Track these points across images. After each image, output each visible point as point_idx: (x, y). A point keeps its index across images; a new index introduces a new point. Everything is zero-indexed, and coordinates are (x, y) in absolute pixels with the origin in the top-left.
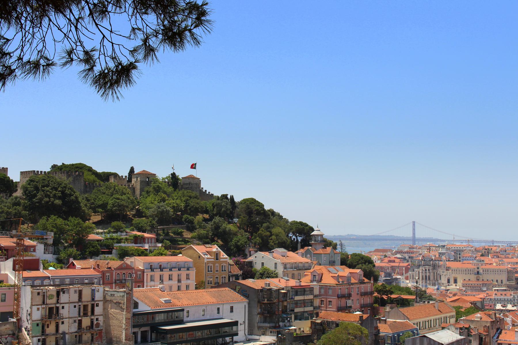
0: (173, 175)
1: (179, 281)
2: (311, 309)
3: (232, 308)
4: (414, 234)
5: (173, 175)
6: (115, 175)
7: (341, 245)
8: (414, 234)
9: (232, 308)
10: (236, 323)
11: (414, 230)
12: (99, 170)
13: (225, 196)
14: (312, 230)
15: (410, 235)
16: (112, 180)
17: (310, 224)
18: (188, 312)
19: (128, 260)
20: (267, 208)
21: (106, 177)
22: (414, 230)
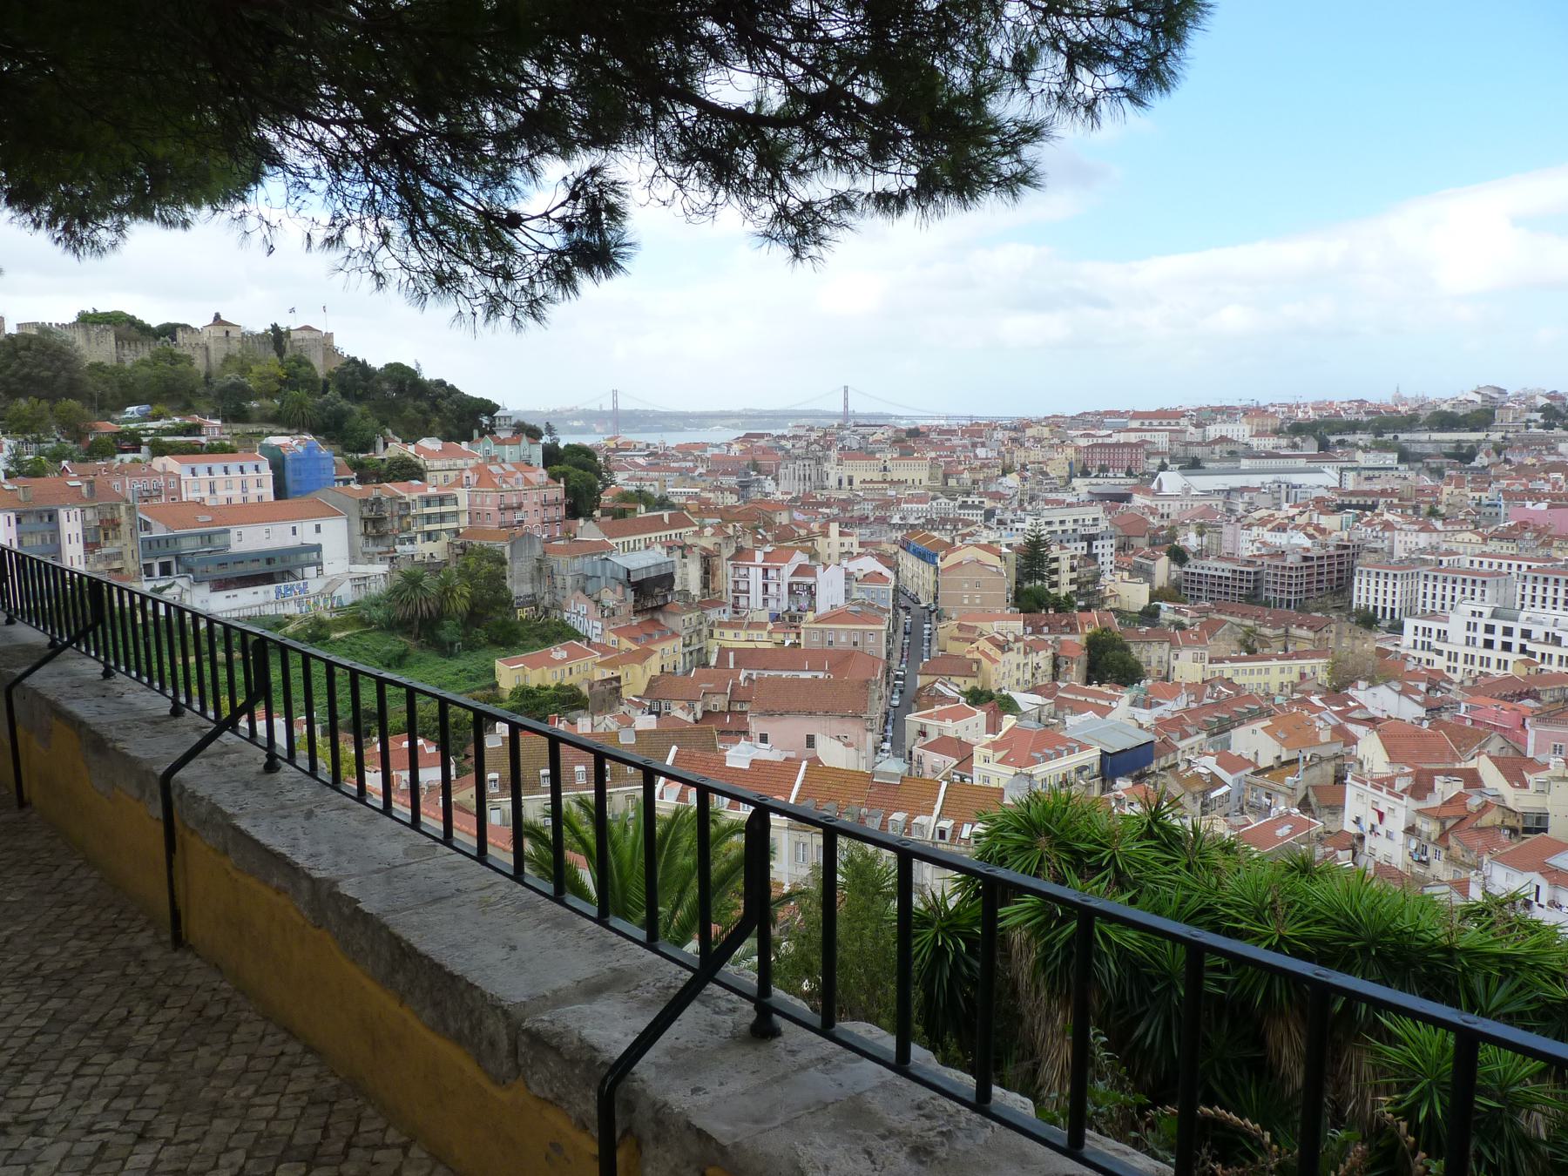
0: (275, 328)
1: (244, 488)
2: (454, 525)
3: (318, 529)
4: (846, 406)
5: (275, 328)
6: (185, 327)
7: (550, 430)
8: (846, 406)
9: (318, 529)
10: (318, 548)
11: (846, 399)
12: (154, 319)
13: (354, 360)
14: (497, 408)
15: (840, 409)
16: (180, 334)
17: (495, 400)
18: (240, 534)
19: (159, 463)
20: (428, 374)
21: (170, 330)
22: (846, 399)
